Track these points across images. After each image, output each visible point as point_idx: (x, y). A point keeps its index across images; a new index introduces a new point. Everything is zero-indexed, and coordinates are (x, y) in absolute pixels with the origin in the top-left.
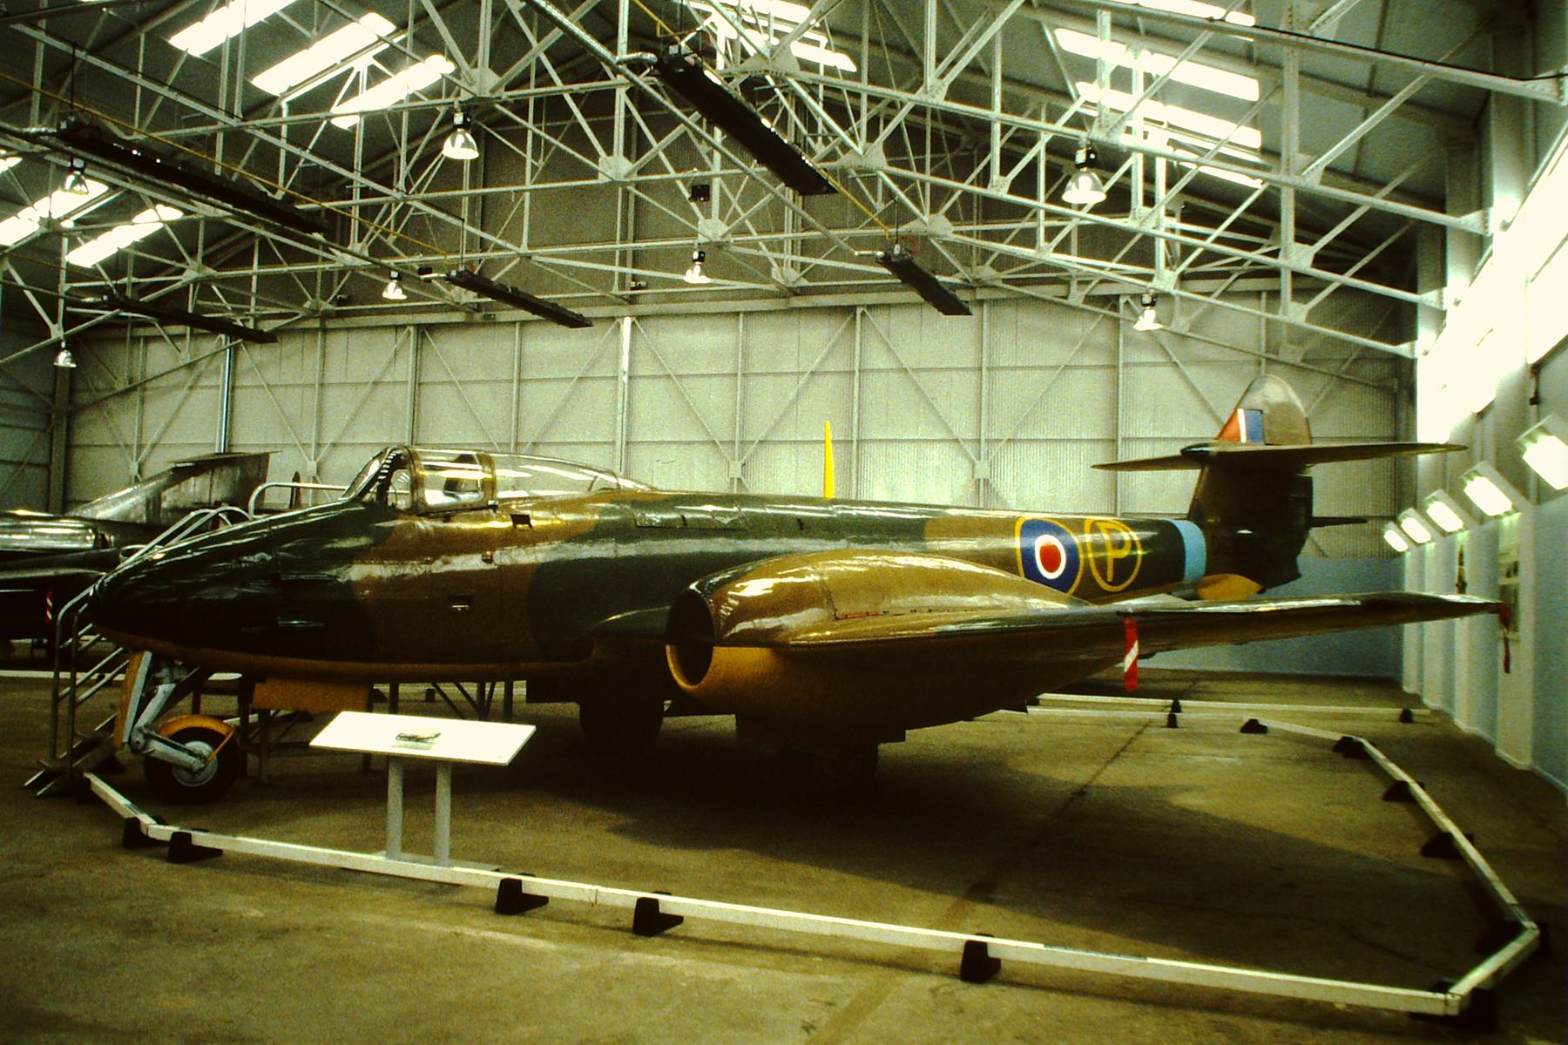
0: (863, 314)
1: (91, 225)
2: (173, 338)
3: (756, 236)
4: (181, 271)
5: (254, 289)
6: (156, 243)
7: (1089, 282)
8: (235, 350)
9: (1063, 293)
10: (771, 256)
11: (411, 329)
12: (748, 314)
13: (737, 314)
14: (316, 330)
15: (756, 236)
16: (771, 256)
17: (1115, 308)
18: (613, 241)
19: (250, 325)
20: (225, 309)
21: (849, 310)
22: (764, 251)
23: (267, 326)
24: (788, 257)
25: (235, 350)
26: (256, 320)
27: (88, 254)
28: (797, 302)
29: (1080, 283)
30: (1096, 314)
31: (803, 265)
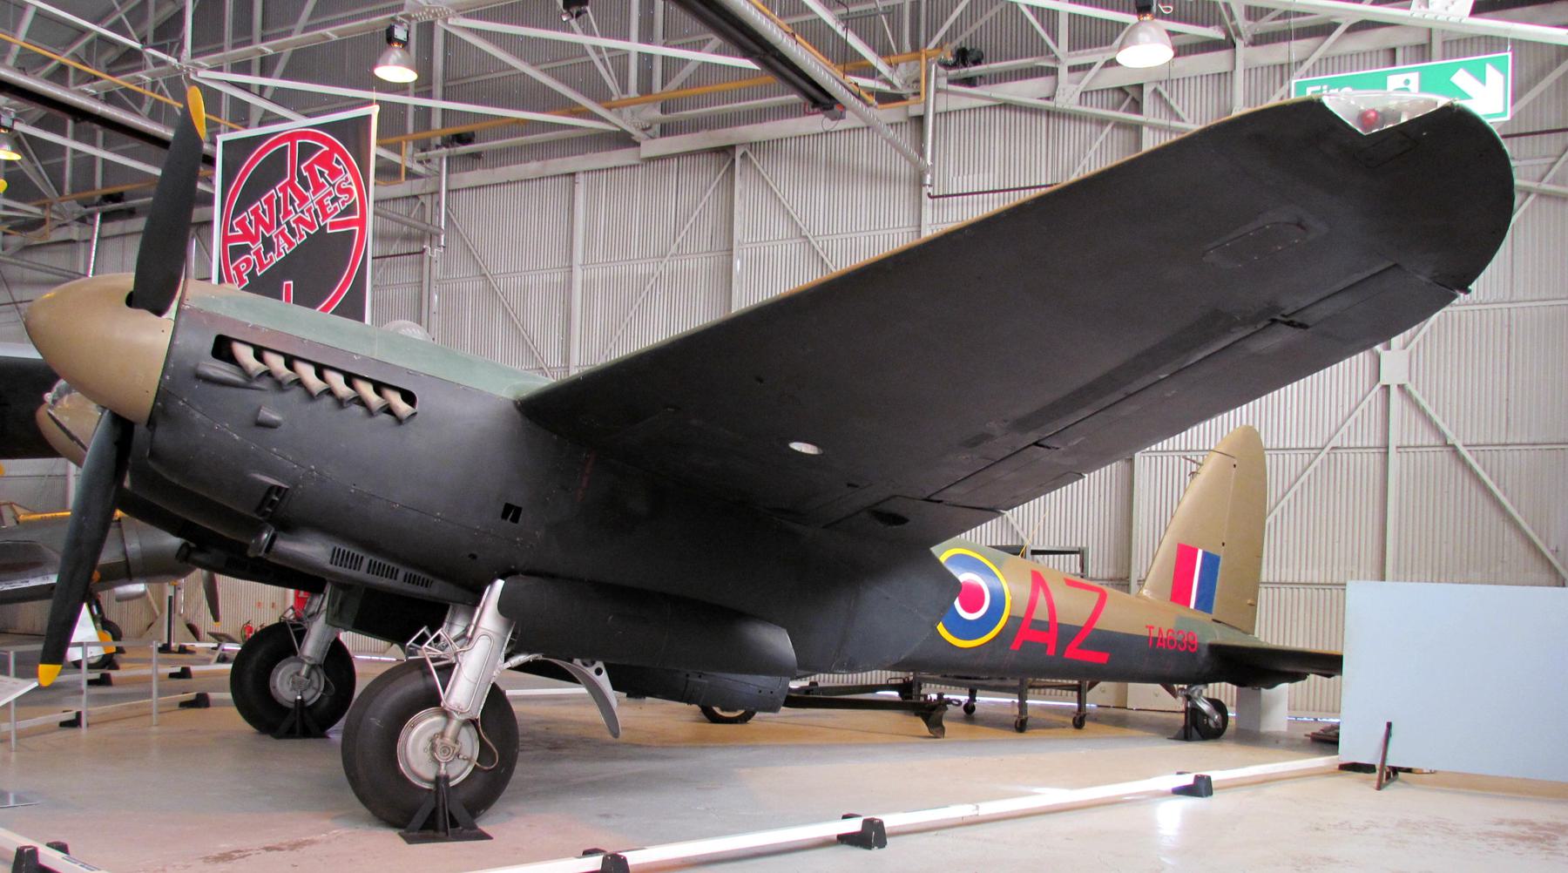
0: (744, 155)
7: (1089, 67)
9: (1045, 94)
17: (1137, 106)
21: (726, 151)
29: (1072, 69)
30: (1102, 122)
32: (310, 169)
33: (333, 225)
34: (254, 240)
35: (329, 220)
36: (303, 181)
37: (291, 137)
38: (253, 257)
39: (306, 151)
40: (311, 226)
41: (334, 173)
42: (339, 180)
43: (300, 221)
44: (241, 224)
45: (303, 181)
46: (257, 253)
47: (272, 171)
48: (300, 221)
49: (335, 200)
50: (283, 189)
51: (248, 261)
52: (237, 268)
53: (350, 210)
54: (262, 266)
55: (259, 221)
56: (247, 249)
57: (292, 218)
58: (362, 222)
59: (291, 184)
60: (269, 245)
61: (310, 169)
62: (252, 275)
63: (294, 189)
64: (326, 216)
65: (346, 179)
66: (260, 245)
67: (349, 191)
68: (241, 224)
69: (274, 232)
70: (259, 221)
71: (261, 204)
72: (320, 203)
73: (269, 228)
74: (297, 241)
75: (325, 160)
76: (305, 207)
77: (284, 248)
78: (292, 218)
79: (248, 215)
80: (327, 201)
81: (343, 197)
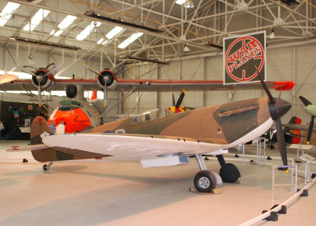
1: (122, 38)
2: (145, 65)
3: (296, 22)
4: (141, 47)
5: (163, 51)
6: (137, 41)
8: (159, 68)
10: (302, 28)
11: (203, 58)
12: (296, 46)
13: (292, 46)
14: (178, 61)
15: (296, 22)
16: (302, 28)
18: (256, 27)
19: (163, 60)
20: (156, 57)
22: (300, 27)
23: (167, 60)
24: (307, 27)
25: (159, 68)
26: (164, 59)
27: (123, 45)
28: (310, 41)
31: (313, 29)
32: (248, 45)
33: (255, 57)
34: (234, 61)
35: (254, 57)
38: (234, 65)
39: (247, 41)
40: (250, 58)
41: (255, 46)
42: (256, 47)
43: (246, 57)
44: (231, 58)
46: (235, 64)
47: (239, 45)
48: (246, 57)
49: (255, 52)
50: (242, 50)
51: (233, 66)
52: (230, 67)
53: (260, 54)
54: (237, 67)
55: (235, 57)
56: (233, 63)
57: (244, 56)
58: (263, 56)
59: (244, 48)
60: (238, 62)
61: (248, 45)
62: (234, 69)
63: (244, 49)
64: (253, 55)
65: (258, 47)
66: (236, 62)
67: (259, 50)
68: (231, 58)
69: (239, 59)
70: (235, 57)
71: (236, 53)
72: (252, 52)
73: (238, 58)
74: (246, 61)
75: (252, 43)
76: (247, 53)
77: (242, 63)
78: (244, 56)
79: (232, 56)
80: (253, 52)
81: (258, 51)
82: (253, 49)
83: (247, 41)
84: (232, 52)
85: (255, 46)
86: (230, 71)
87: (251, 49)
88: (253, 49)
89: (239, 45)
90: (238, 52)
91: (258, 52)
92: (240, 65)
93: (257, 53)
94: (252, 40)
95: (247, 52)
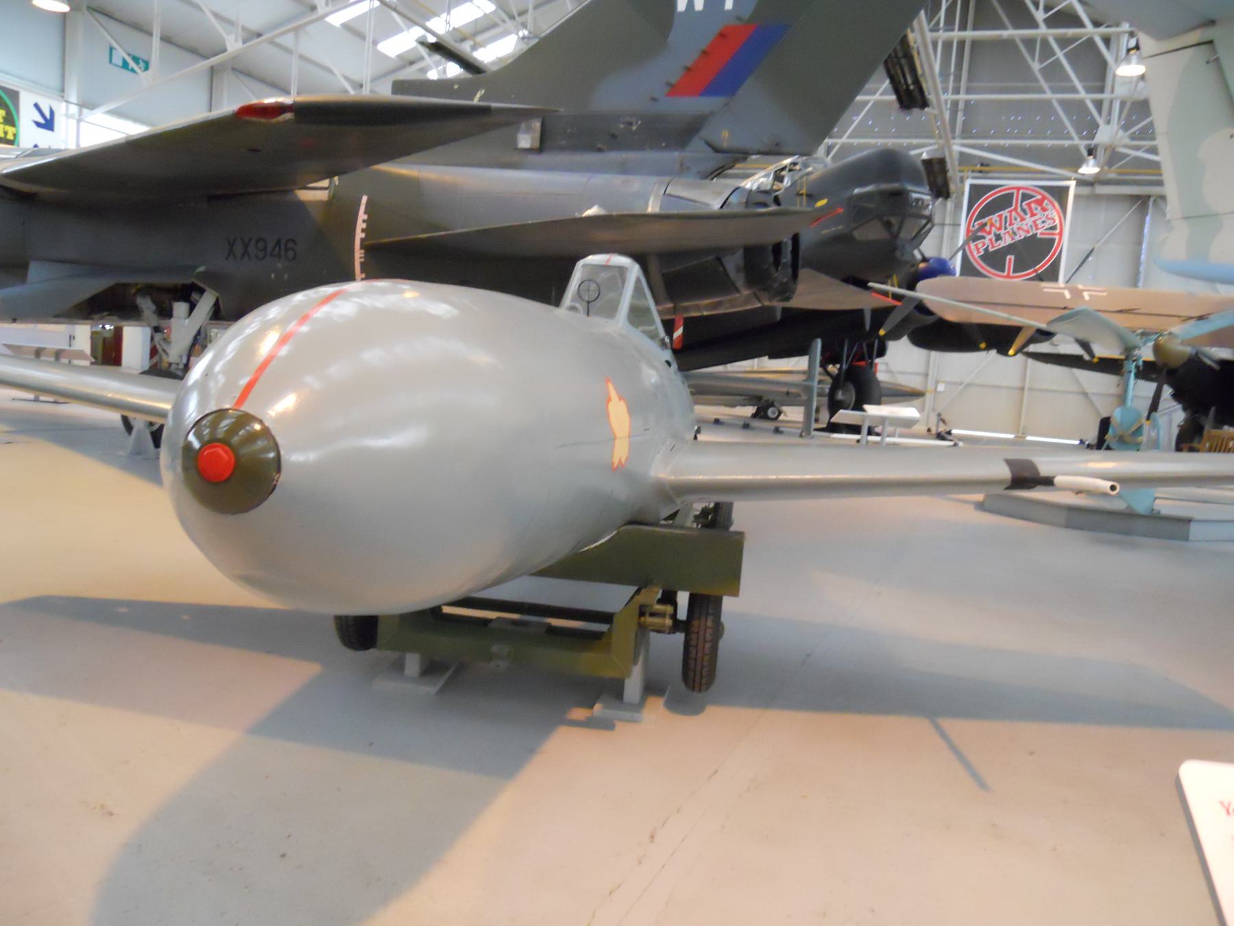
32: (1029, 205)
34: (989, 233)
36: (1024, 211)
37: (1018, 189)
39: (1026, 197)
41: (1044, 210)
45: (1024, 211)
47: (1004, 202)
53: (1053, 228)
55: (992, 225)
56: (983, 238)
57: (1015, 227)
59: (1016, 209)
60: (998, 237)
61: (1029, 205)
62: (986, 250)
66: (992, 236)
71: (995, 217)
73: (1000, 229)
74: (1017, 238)
75: (1040, 202)
77: (1007, 240)
78: (1015, 227)
80: (1039, 222)
82: (1040, 215)
83: (1026, 197)
84: (983, 214)
85: (1044, 210)
86: (975, 253)
87: (1033, 215)
88: (1040, 215)
89: (1004, 202)
90: (1000, 216)
91: (1048, 224)
92: (1002, 244)
93: (1047, 225)
94: (1039, 197)
95: (1023, 219)
